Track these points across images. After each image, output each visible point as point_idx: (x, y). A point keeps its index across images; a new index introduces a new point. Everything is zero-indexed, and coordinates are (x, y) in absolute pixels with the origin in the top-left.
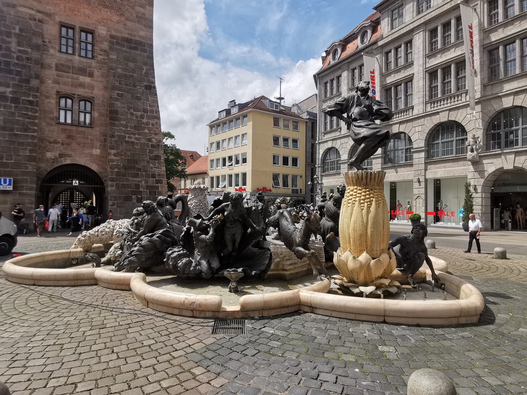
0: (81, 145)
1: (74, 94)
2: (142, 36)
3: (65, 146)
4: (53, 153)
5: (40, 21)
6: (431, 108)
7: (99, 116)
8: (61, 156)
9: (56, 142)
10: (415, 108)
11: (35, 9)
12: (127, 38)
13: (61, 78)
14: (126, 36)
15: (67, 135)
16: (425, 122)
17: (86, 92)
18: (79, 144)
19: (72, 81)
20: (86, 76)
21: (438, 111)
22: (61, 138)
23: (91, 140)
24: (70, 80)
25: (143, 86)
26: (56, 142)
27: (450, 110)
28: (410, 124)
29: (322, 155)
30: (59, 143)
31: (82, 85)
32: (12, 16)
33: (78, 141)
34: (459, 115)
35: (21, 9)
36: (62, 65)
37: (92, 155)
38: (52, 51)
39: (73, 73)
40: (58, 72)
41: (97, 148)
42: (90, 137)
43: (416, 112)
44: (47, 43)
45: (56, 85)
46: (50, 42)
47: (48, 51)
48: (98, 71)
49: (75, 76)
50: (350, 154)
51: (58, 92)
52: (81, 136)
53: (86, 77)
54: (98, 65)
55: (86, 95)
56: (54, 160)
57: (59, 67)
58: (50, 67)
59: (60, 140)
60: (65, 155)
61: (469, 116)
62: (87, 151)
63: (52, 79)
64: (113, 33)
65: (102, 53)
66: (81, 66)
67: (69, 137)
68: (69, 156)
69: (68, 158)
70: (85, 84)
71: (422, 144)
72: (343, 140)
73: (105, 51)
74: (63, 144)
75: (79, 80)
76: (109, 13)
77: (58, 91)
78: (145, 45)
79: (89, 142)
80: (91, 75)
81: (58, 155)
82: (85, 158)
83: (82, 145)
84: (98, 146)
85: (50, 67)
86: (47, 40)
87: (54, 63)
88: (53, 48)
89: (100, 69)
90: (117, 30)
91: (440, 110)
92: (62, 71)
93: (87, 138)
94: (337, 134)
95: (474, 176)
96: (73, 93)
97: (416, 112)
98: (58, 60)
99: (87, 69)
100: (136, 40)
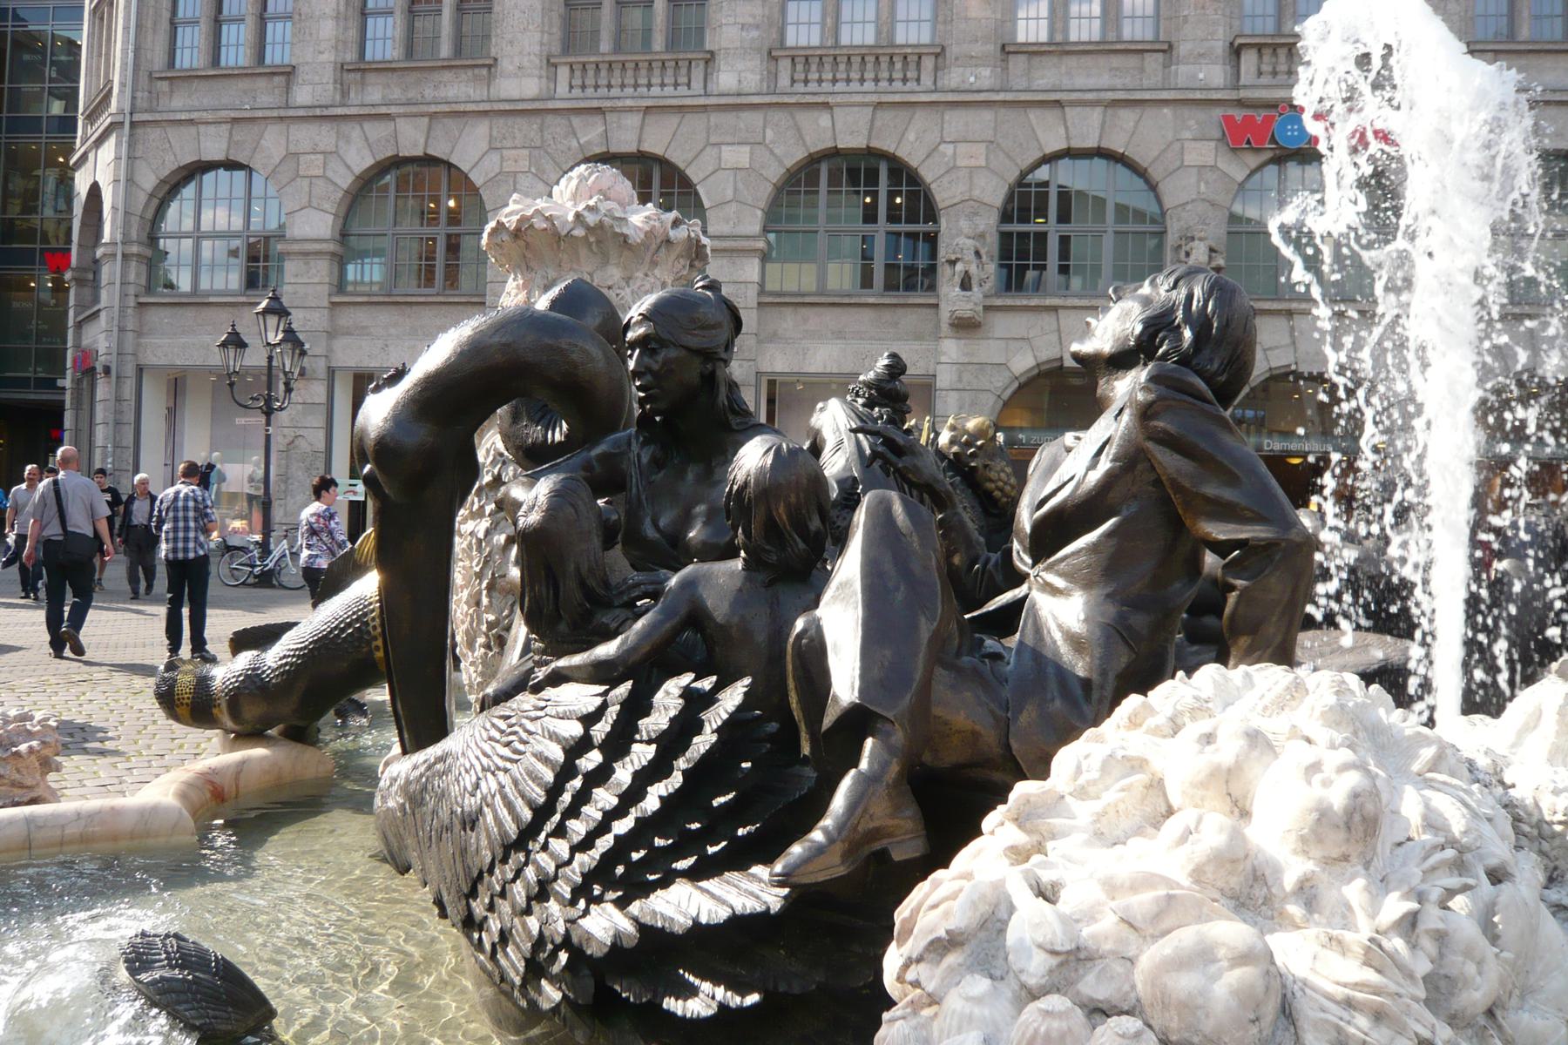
6: (793, 81)
10: (721, 62)
16: (769, 134)
21: (830, 99)
27: (879, 105)
28: (696, 123)
29: (152, 195)
34: (911, 136)
43: (726, 79)
50: (342, 214)
61: (948, 149)
71: (752, 223)
72: (305, 136)
91: (1074, 96)
94: (265, 95)
95: (960, 380)
97: (726, 79)
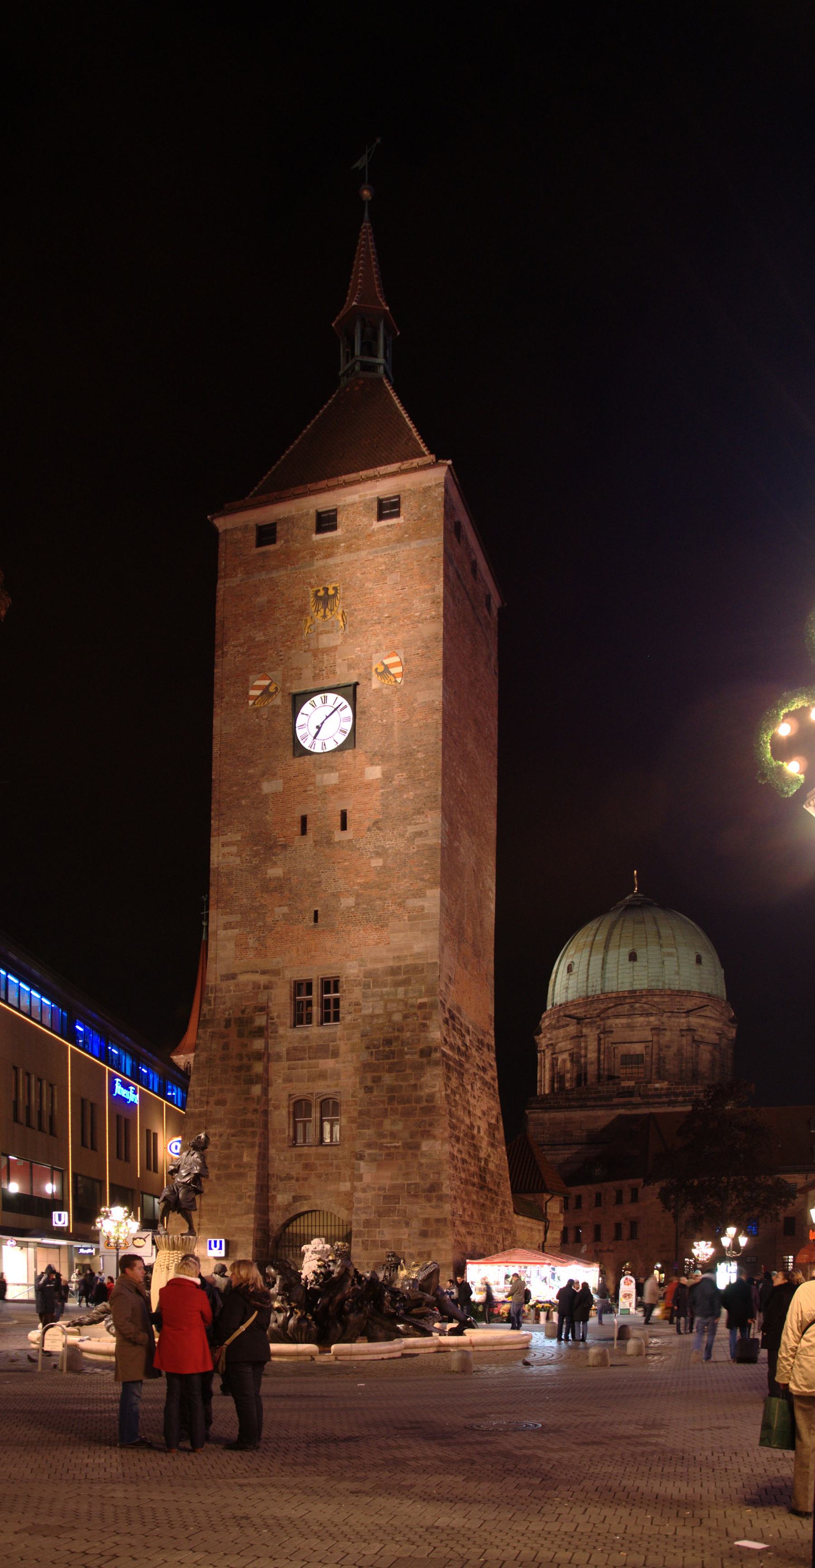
0: (323, 1178)
1: (312, 1094)
2: (419, 954)
3: (301, 1182)
4: (285, 1196)
5: (266, 987)
7: (348, 1122)
8: (296, 1199)
9: (289, 1177)
11: (259, 970)
12: (392, 968)
13: (294, 1071)
14: (391, 963)
15: (303, 1164)
17: (328, 1086)
18: (319, 1176)
19: (308, 1072)
20: (327, 1058)
22: (296, 1170)
23: (338, 1167)
24: (305, 1071)
25: (415, 1053)
26: (289, 1177)
30: (292, 1178)
31: (323, 1075)
32: (232, 993)
33: (318, 1171)
35: (242, 978)
36: (295, 1049)
37: (339, 1193)
38: (281, 1031)
39: (310, 1058)
40: (289, 1063)
41: (345, 1181)
42: (335, 1162)
44: (276, 1020)
45: (288, 1085)
46: (279, 1017)
47: (276, 1032)
48: (346, 1044)
49: (313, 1061)
51: (290, 1095)
52: (322, 1162)
53: (327, 1060)
54: (345, 1032)
55: (328, 1090)
56: (287, 1208)
57: (294, 1054)
58: (279, 1057)
59: (293, 1173)
60: (301, 1197)
62: (331, 1187)
63: (282, 1076)
64: (370, 966)
65: (352, 1009)
66: (321, 1043)
67: (307, 1166)
68: (307, 1198)
69: (305, 1202)
70: (327, 1072)
73: (357, 1004)
74: (297, 1180)
75: (318, 1067)
76: (362, 932)
77: (291, 1093)
78: (423, 969)
79: (334, 1171)
80: (335, 1054)
81: (291, 1198)
82: (330, 1199)
83: (324, 1177)
84: (347, 1176)
85: (279, 1057)
86: (275, 1014)
87: (284, 1049)
88: (283, 1024)
89: (348, 1040)
90: (376, 960)
92: (295, 1060)
93: (332, 1164)
96: (310, 1091)
98: (290, 1043)
99: (328, 1045)
100: (407, 966)
